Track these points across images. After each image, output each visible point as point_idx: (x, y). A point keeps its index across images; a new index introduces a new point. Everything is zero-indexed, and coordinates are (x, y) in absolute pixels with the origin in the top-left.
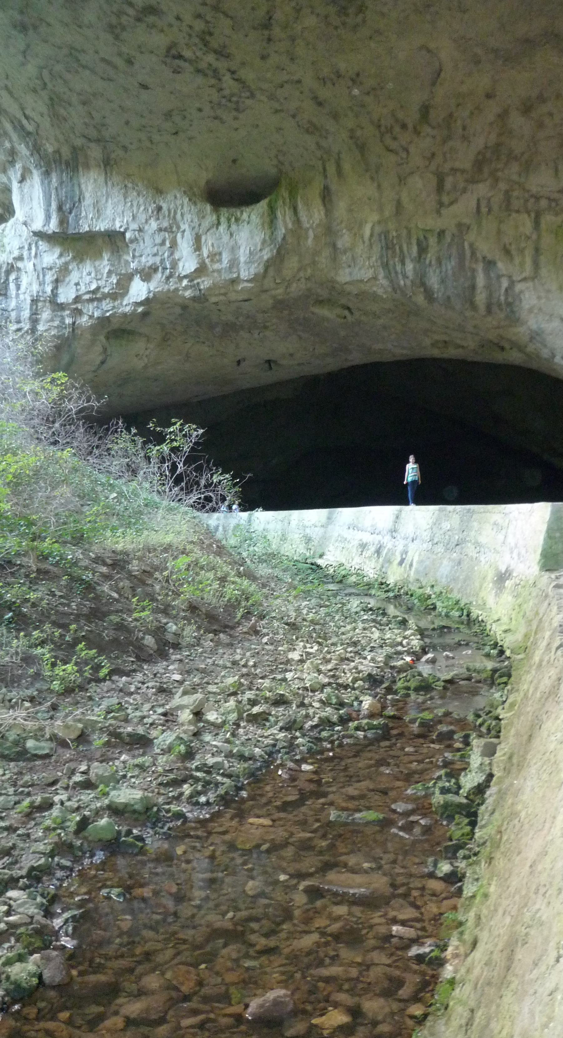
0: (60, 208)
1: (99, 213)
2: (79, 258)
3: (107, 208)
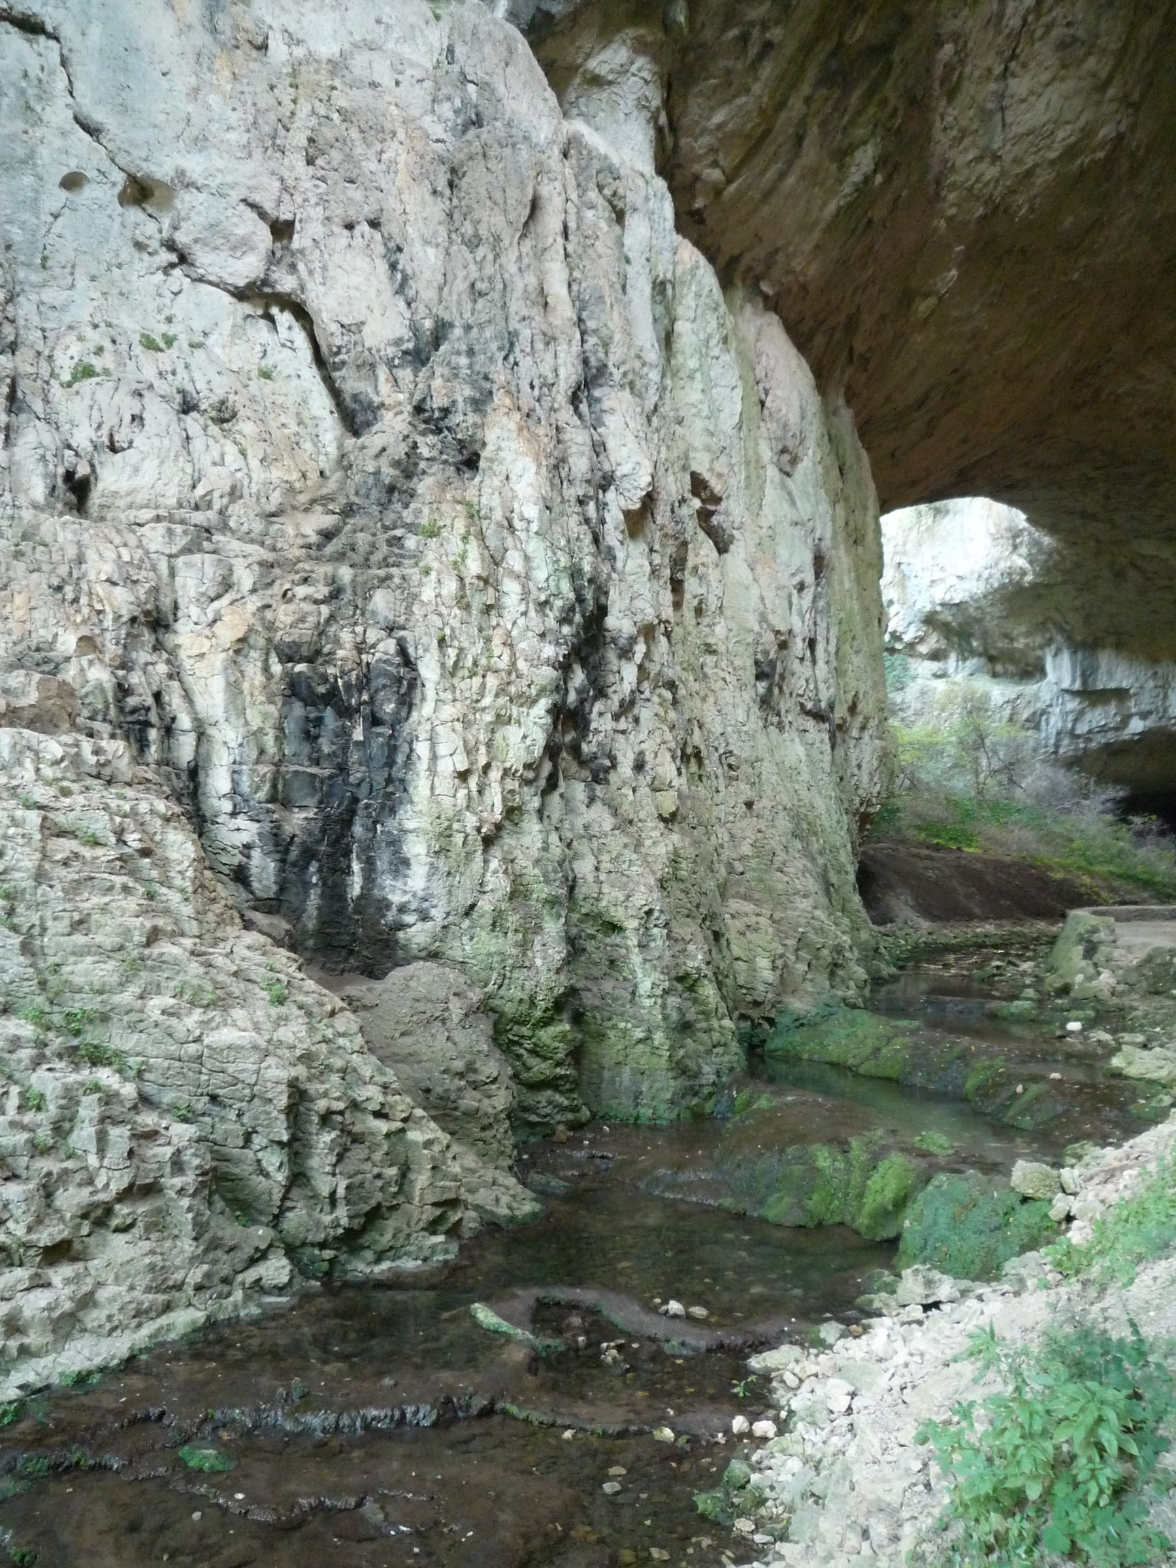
0: (1083, 675)
1: (1110, 674)
2: (1093, 704)
3: (1115, 673)
